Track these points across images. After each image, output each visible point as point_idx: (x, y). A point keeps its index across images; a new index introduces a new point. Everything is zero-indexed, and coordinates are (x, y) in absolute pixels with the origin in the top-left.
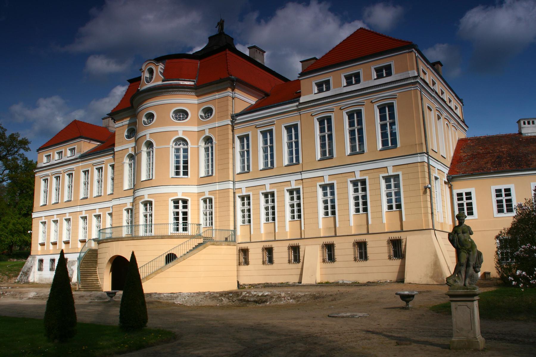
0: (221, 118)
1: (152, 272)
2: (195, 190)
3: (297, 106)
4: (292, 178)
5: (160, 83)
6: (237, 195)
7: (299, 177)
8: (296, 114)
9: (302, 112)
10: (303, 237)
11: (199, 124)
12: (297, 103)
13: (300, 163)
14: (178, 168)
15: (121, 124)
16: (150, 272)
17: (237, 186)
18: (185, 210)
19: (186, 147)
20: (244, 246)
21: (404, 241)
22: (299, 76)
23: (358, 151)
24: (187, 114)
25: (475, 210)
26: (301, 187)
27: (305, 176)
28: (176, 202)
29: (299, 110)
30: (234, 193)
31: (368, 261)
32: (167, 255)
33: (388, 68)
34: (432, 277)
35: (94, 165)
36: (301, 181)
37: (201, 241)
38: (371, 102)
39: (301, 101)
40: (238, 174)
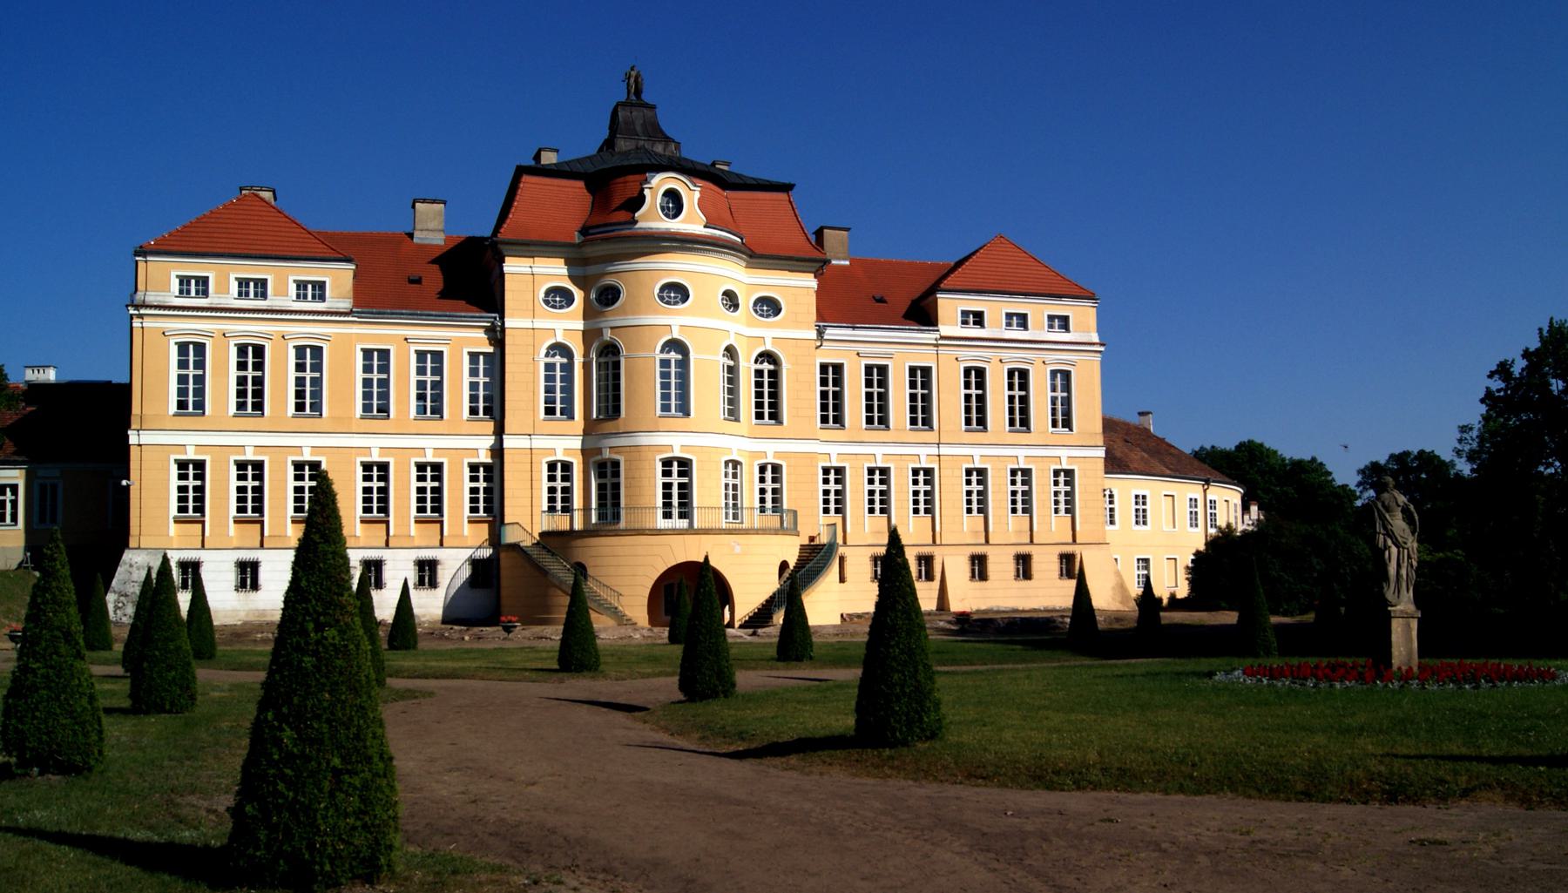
0: (797, 324)
3: (936, 340)
4: (923, 451)
7: (934, 450)
9: (940, 348)
10: (938, 542)
11: (750, 324)
13: (935, 428)
14: (759, 405)
26: (936, 467)
27: (944, 450)
29: (937, 345)
31: (1032, 581)
34: (1121, 603)
35: (409, 341)
38: (1044, 362)
39: (943, 334)
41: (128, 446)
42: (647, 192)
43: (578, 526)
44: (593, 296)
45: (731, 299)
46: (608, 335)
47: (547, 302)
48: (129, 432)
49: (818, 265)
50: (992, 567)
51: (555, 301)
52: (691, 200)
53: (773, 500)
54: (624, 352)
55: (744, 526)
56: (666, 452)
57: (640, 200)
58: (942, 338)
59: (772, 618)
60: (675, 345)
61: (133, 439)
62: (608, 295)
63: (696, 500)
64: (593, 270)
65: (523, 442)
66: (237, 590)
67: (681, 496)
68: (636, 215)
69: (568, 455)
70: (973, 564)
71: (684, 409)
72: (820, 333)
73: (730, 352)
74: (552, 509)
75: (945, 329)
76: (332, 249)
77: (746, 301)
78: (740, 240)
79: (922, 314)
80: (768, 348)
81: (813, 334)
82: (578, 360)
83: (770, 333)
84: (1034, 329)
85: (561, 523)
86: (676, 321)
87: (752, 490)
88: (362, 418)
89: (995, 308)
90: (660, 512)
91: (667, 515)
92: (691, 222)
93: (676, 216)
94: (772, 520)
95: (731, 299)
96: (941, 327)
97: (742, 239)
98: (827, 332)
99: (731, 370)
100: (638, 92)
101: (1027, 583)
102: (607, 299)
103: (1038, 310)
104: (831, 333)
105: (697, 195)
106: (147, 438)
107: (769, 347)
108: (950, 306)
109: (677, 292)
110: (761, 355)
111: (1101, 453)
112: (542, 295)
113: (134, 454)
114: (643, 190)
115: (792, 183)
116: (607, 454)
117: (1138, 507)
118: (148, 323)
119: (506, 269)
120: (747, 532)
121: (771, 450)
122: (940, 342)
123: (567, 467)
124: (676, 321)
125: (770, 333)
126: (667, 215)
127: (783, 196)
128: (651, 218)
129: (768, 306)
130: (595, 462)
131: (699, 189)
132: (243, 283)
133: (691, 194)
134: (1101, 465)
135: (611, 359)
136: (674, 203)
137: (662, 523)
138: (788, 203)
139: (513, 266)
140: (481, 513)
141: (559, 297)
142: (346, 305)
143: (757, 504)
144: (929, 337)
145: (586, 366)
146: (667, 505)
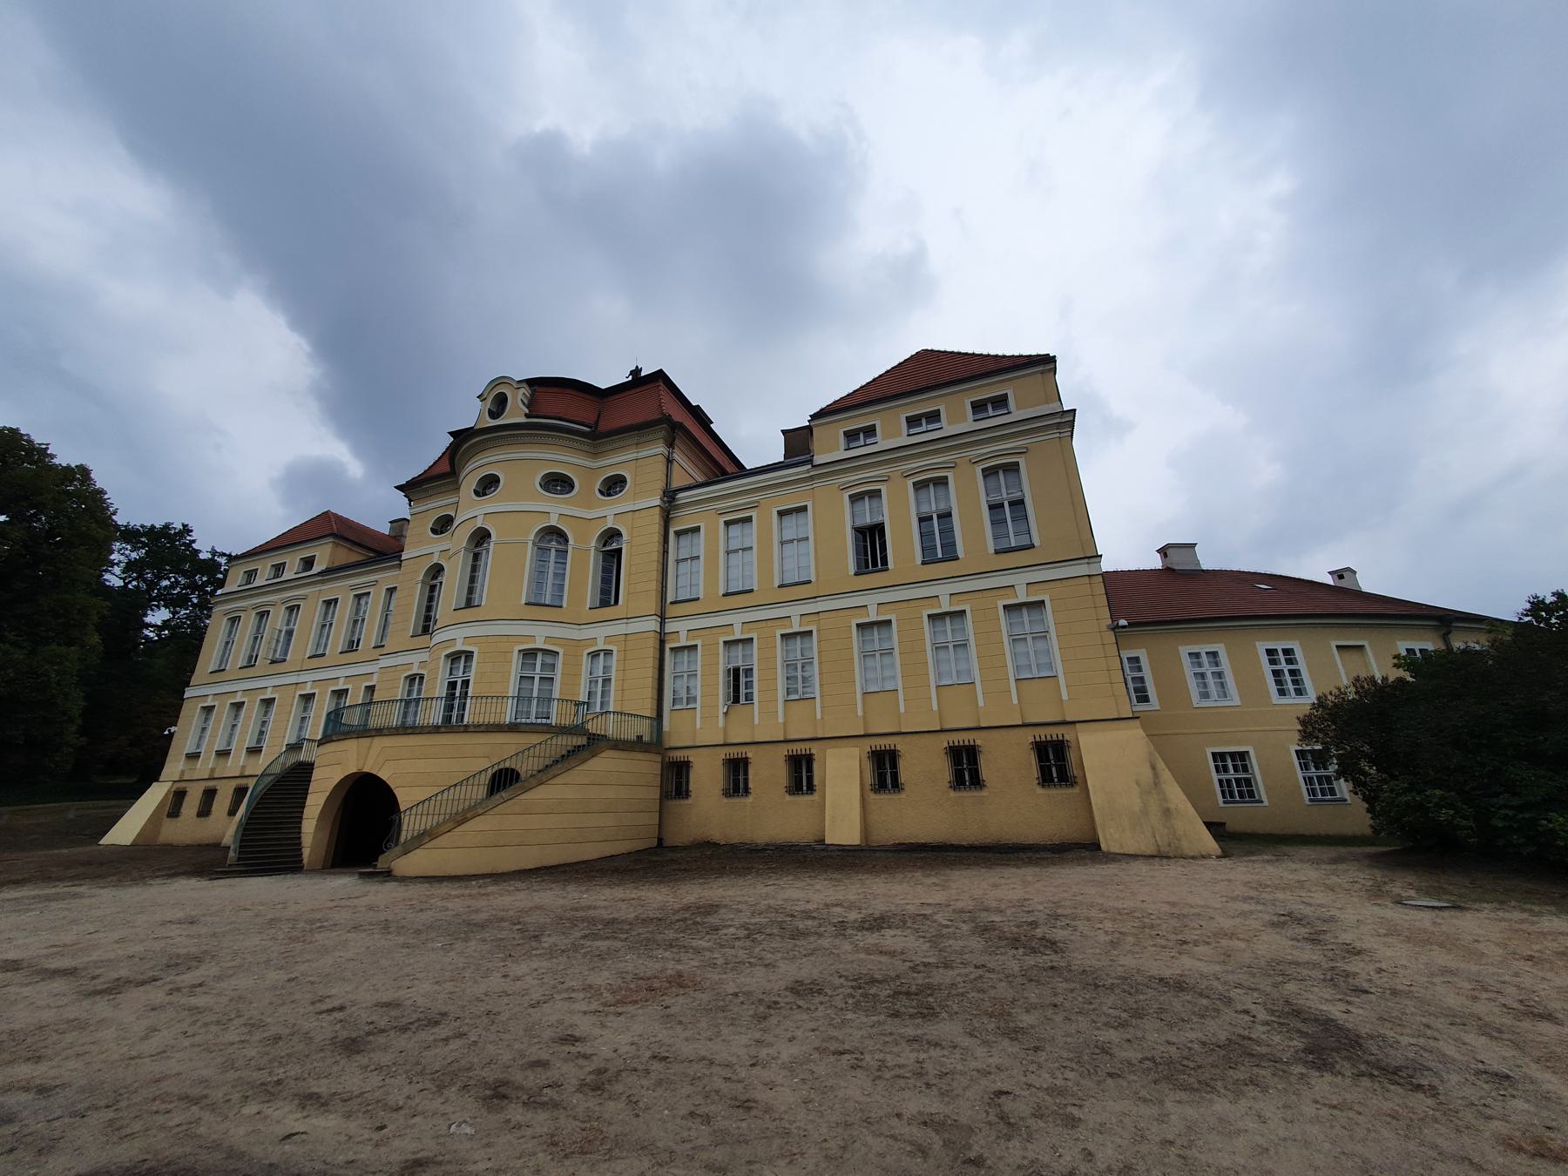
1: (423, 827)
3: (808, 471)
5: (523, 420)
6: (668, 646)
12: (810, 466)
16: (417, 827)
18: (547, 674)
19: (561, 547)
22: (810, 418)
23: (940, 556)
24: (572, 486)
25: (1152, 692)
28: (529, 654)
29: (812, 478)
32: (494, 775)
33: (1001, 402)
37: (582, 741)
39: (816, 463)
40: (671, 603)
52: (515, 398)
75: (818, 460)
122: (812, 473)
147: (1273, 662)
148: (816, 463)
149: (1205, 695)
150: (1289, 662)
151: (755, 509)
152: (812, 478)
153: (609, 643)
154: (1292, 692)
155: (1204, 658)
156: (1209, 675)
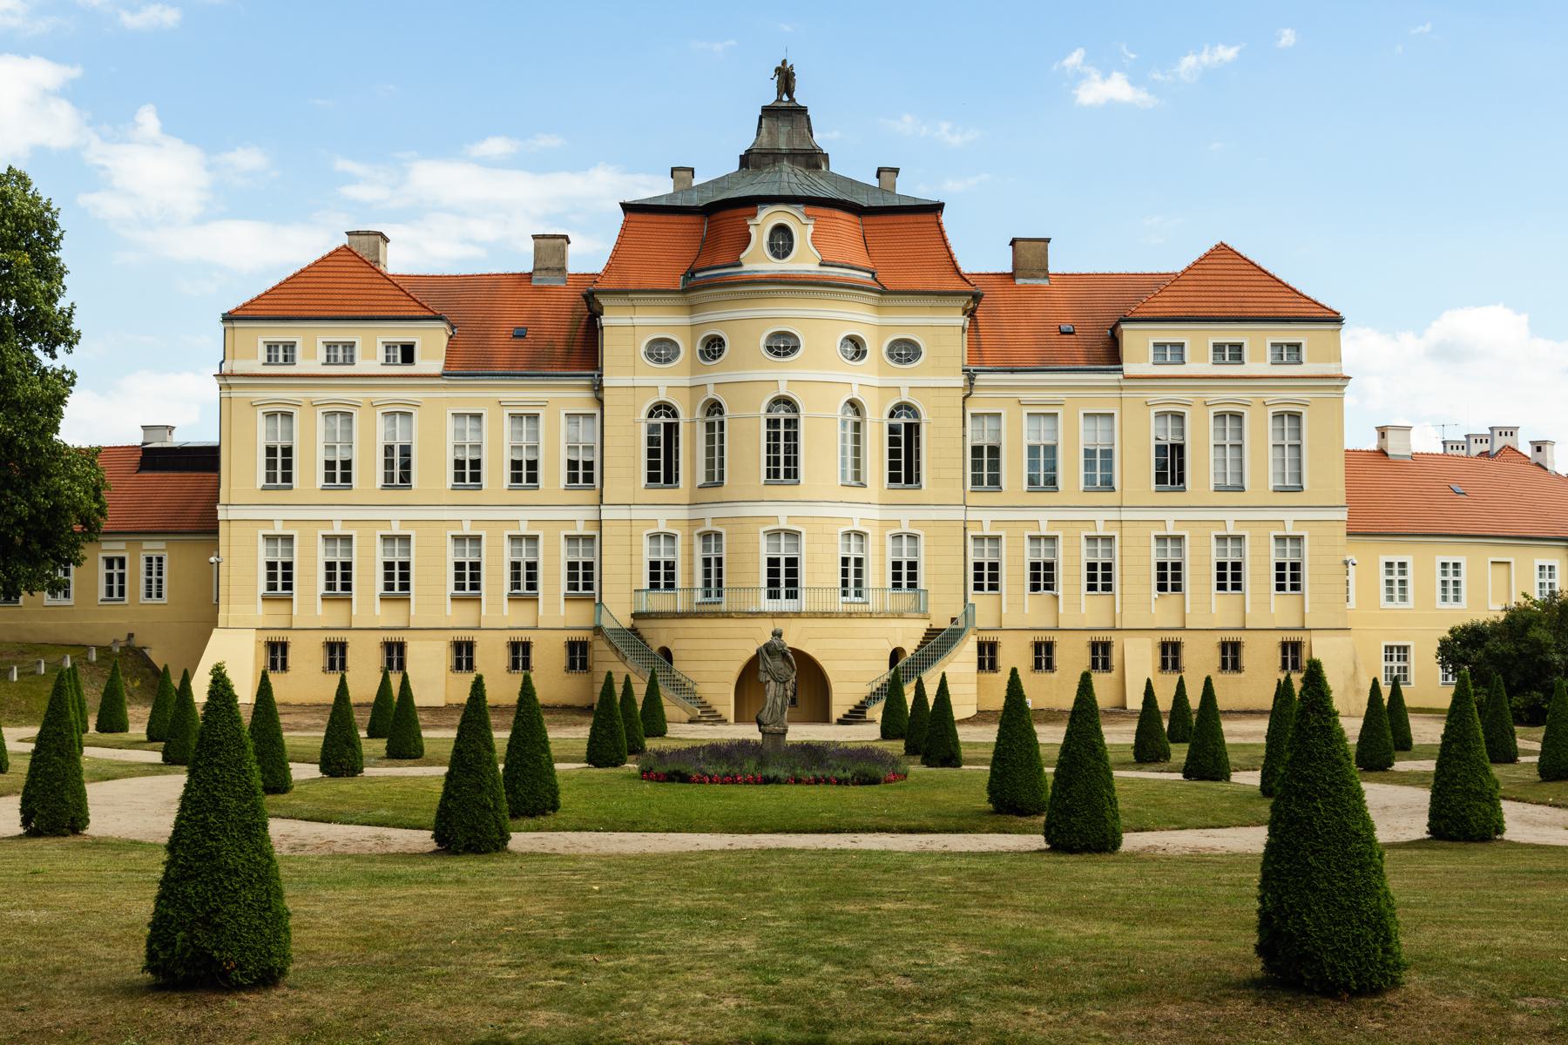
2: (875, 513)
3: (1119, 380)
4: (1100, 516)
6: (970, 533)
7: (1114, 515)
8: (1115, 393)
9: (1125, 394)
12: (1121, 377)
15: (628, 322)
17: (973, 515)
20: (988, 636)
21: (1307, 645)
27: (1126, 515)
29: (1121, 388)
30: (965, 529)
31: (1243, 675)
36: (1118, 524)
39: (1126, 372)
41: (217, 522)
42: (752, 230)
43: (680, 608)
44: (698, 347)
45: (856, 347)
46: (711, 393)
47: (650, 355)
48: (218, 507)
49: (962, 302)
50: (1246, 658)
51: (660, 355)
53: (905, 575)
54: (727, 412)
55: (870, 608)
56: (770, 524)
57: (746, 240)
58: (1126, 378)
59: (864, 713)
60: (787, 402)
61: (222, 514)
62: (714, 346)
63: (804, 579)
64: (699, 319)
65: (623, 513)
66: (324, 671)
67: (788, 573)
68: (741, 256)
69: (671, 527)
70: (1284, 652)
71: (792, 474)
72: (971, 378)
73: (854, 405)
74: (655, 586)
75: (1130, 368)
76: (423, 306)
77: (876, 347)
78: (870, 275)
79: (1111, 354)
80: (903, 400)
81: (960, 381)
82: (683, 419)
83: (907, 382)
84: (1252, 360)
85: (660, 601)
86: (784, 376)
87: (883, 565)
88: (454, 488)
89: (1199, 341)
90: (764, 593)
91: (773, 595)
92: (804, 260)
93: (786, 255)
94: (905, 598)
95: (856, 347)
96: (1125, 365)
97: (873, 274)
98: (977, 377)
99: (857, 426)
100: (790, 93)
101: (1235, 676)
102: (714, 351)
103: (1258, 342)
104: (980, 376)
105: (810, 229)
106: (233, 514)
107: (905, 397)
108: (1138, 343)
109: (783, 345)
110: (899, 407)
111: (1343, 515)
112: (643, 349)
113: (223, 527)
114: (749, 226)
115: (941, 201)
116: (709, 527)
117: (1542, 580)
118: (235, 393)
119: (606, 320)
120: (870, 615)
121: (906, 519)
123: (671, 538)
124: (784, 376)
125: (907, 382)
126: (776, 255)
127: (930, 218)
128: (758, 260)
129: (904, 351)
130: (699, 534)
131: (813, 222)
132: (330, 346)
133: (803, 228)
134: (1342, 530)
135: (716, 418)
136: (782, 240)
137: (768, 605)
138: (936, 225)
139: (613, 319)
140: (581, 591)
141: (662, 351)
142: (437, 366)
143: (889, 582)
144: (1112, 378)
145: (693, 422)
146: (773, 583)
147: (1444, 573)
148: (1126, 372)
149: (1391, 599)
150: (1456, 573)
151: (1062, 408)
152: (1121, 388)
153: (915, 527)
154: (1452, 598)
155: (1396, 568)
156: (1396, 583)
